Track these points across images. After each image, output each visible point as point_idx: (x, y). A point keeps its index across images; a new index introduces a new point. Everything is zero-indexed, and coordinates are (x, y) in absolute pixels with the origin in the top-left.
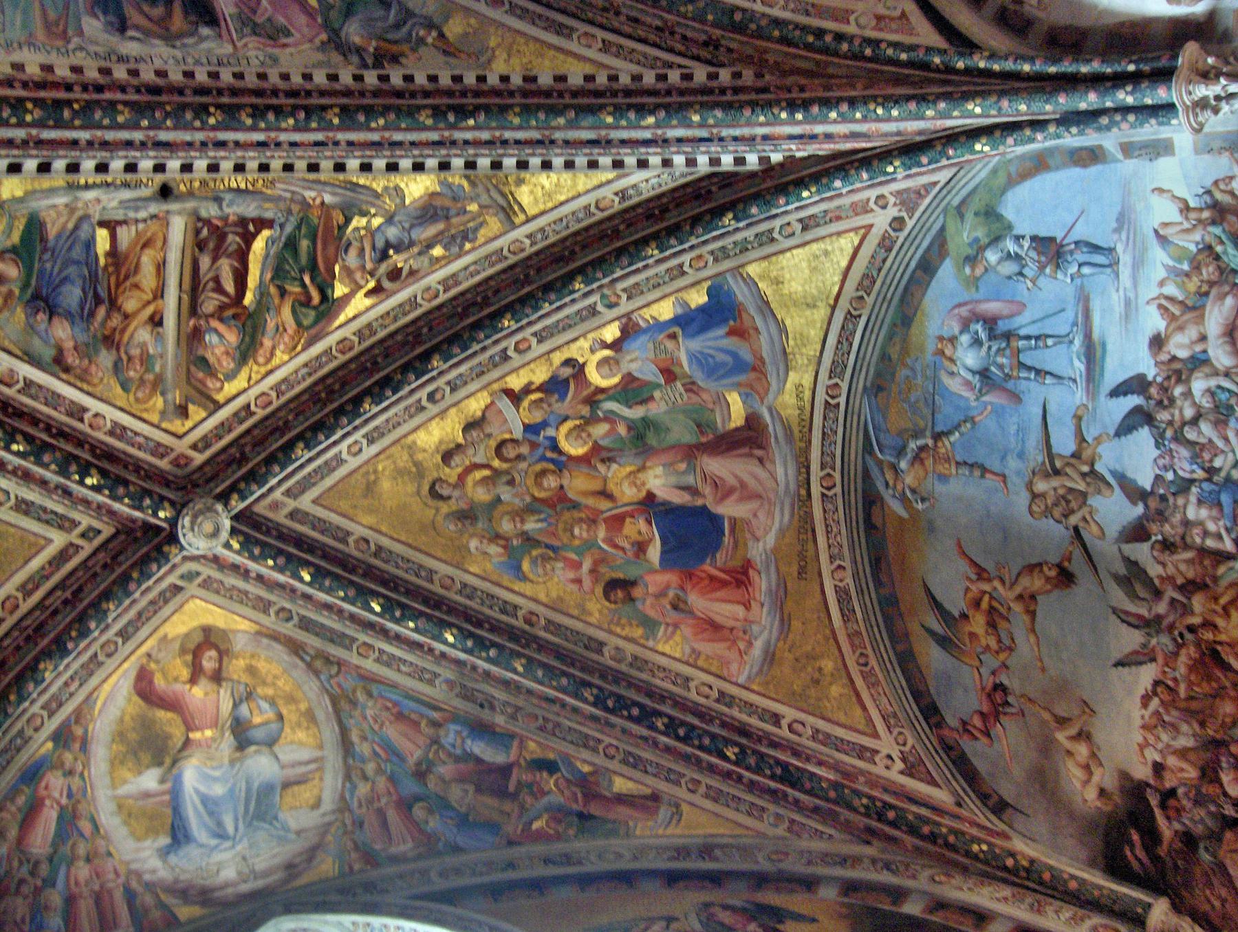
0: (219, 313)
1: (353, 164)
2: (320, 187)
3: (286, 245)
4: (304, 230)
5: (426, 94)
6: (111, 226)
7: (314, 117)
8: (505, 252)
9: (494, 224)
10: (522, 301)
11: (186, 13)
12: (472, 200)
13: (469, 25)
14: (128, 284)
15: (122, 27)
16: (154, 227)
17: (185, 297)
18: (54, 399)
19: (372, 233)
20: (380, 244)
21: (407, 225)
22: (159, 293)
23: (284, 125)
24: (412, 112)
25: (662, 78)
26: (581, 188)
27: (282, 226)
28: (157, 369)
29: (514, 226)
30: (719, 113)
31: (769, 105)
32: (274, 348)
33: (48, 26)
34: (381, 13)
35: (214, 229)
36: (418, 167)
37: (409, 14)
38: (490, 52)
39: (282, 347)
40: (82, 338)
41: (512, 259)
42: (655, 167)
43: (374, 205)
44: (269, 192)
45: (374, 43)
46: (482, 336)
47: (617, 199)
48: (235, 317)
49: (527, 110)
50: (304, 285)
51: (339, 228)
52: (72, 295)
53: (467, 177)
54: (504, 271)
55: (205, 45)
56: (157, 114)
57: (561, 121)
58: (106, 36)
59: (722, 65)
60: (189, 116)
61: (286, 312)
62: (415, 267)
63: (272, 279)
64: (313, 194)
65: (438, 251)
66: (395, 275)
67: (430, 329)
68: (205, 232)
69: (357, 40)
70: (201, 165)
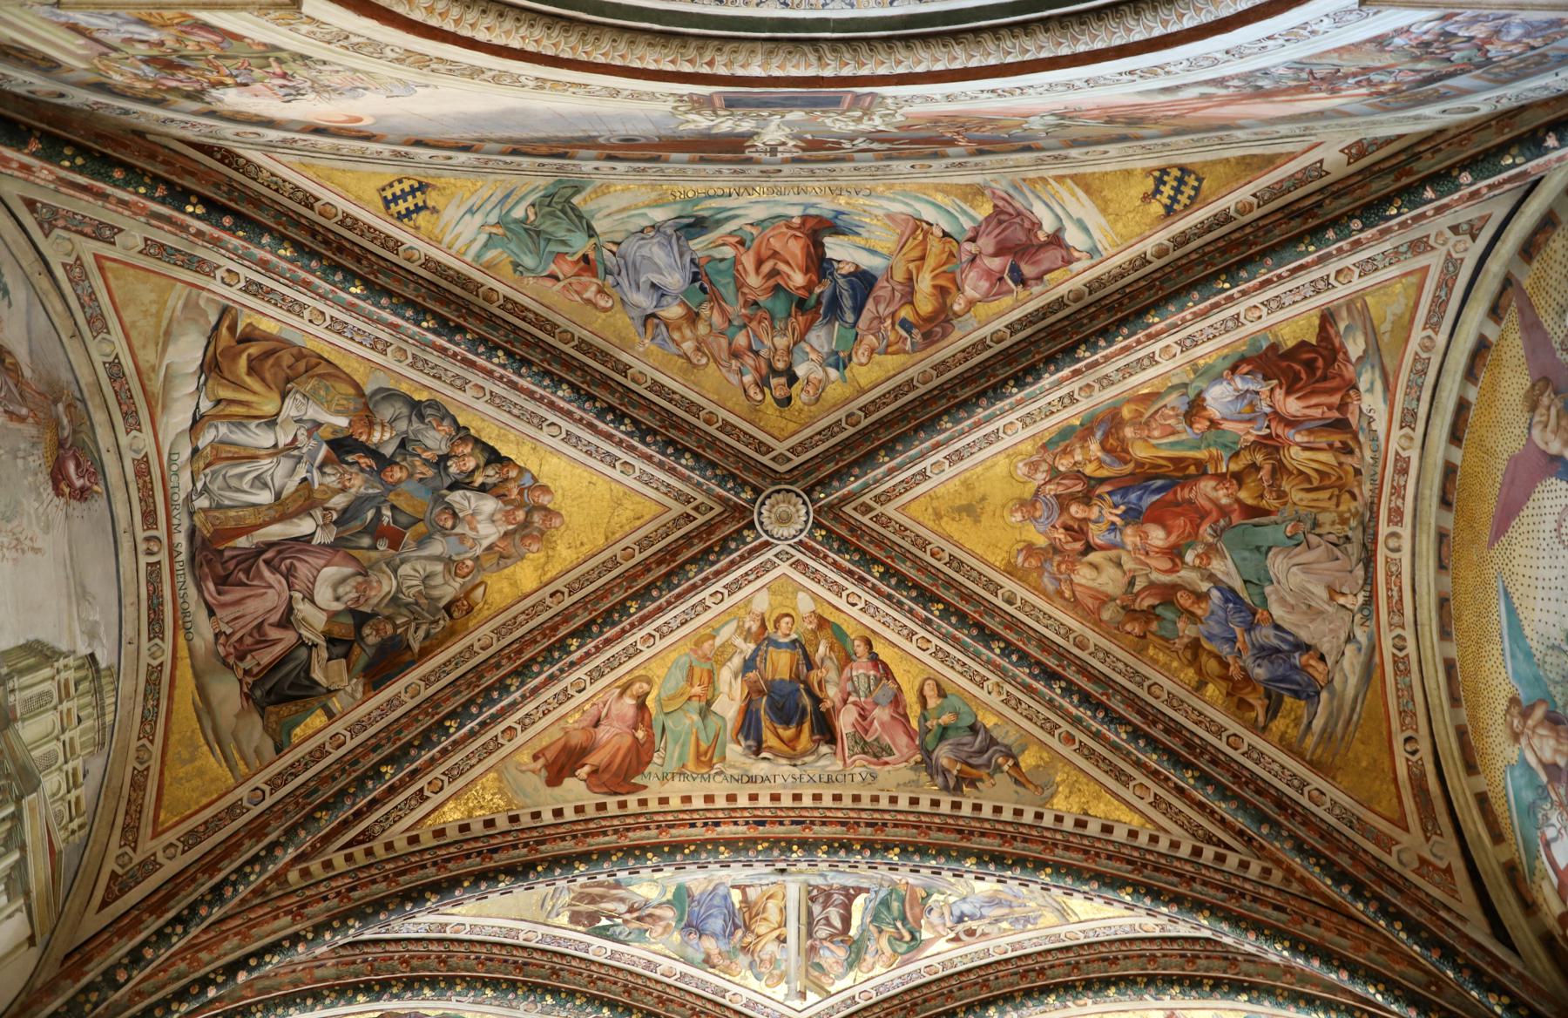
6: (742, 888)
9: (1050, 918)
11: (812, 732)
18: (704, 984)
19: (950, 906)
20: (957, 913)
22: (783, 924)
25: (1197, 852)
29: (1068, 922)
33: (698, 755)
34: (969, 739)
37: (992, 742)
40: (724, 948)
45: (959, 766)
52: (716, 924)
55: (822, 763)
58: (743, 759)
61: (884, 943)
65: (1004, 925)
66: (971, 933)
69: (944, 762)
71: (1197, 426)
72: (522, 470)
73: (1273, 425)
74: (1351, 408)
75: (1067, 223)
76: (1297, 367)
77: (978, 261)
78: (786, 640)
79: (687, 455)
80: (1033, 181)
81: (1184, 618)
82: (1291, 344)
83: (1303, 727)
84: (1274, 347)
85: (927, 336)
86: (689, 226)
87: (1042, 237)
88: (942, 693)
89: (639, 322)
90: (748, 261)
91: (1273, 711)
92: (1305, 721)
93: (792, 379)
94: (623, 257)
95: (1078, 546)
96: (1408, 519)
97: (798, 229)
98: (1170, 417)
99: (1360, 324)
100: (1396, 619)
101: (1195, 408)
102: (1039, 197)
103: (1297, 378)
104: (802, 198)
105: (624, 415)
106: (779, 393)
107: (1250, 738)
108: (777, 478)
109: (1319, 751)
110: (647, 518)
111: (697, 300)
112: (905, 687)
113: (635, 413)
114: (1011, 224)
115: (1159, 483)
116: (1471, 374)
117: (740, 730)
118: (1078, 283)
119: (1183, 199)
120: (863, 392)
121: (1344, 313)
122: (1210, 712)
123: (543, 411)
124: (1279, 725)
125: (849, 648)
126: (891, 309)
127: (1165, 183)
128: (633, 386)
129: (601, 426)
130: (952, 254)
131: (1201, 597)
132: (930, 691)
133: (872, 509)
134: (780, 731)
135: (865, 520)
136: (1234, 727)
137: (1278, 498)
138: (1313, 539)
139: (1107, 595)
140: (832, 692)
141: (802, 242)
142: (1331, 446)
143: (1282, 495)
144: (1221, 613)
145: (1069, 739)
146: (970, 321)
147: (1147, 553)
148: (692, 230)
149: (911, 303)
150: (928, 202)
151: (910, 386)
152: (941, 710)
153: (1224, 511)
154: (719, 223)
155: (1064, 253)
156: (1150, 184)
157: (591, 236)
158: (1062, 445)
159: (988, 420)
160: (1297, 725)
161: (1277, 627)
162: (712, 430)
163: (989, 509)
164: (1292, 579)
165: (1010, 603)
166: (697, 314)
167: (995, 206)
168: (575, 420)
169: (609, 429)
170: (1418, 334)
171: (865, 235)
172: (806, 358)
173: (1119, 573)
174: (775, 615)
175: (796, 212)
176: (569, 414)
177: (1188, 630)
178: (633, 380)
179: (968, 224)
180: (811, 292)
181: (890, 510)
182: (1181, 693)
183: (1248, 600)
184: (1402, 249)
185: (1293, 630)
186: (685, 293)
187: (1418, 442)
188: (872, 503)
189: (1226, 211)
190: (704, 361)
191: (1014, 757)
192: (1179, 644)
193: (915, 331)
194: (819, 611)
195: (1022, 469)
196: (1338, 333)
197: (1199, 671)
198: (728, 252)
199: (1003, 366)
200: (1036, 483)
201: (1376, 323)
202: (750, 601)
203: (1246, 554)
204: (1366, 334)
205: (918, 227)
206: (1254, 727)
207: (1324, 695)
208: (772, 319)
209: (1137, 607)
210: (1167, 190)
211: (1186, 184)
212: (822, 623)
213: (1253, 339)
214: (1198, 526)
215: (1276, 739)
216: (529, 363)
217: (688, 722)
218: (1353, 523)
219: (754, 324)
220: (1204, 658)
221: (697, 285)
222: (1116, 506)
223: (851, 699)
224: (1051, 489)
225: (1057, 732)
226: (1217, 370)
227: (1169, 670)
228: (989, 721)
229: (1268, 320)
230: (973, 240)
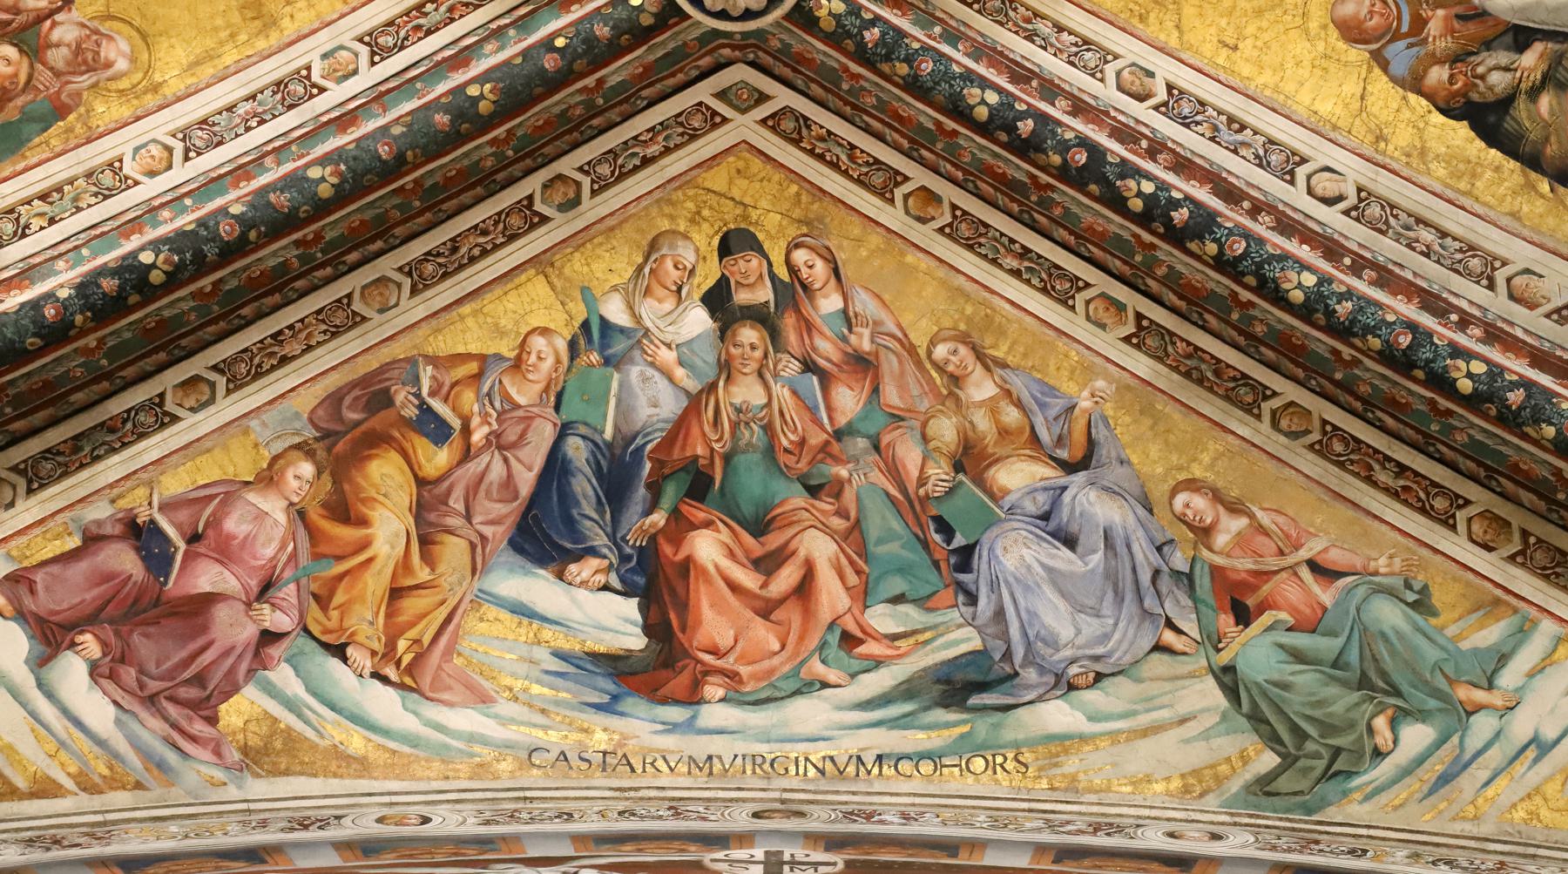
72: (1414, 83)
75: (24, 678)
77: (254, 584)
79: (982, 113)
85: (382, 400)
86: (983, 687)
87: (90, 643)
89: (1104, 452)
90: (832, 596)
93: (717, 300)
94: (1146, 614)
97: (710, 671)
102: (101, 743)
104: (701, 746)
105: (1143, 219)
108: (754, 50)
111: (958, 501)
113: (1115, 223)
114: (169, 675)
123: (1355, 234)
126: (474, 467)
128: (1120, 292)
129: (1203, 194)
130: (323, 601)
141: (701, 638)
146: (270, 436)
148: (973, 675)
149: (421, 482)
154: (906, 691)
155: (28, 602)
157: (1229, 669)
162: (920, 177)
166: (958, 467)
167: (213, 720)
168: (1271, 209)
169: (1182, 186)
171: (542, 654)
175: (715, 714)
176: (1287, 226)
178: (1120, 307)
179: (283, 675)
180: (675, 514)
186: (991, 522)
190: (941, 351)
193: (411, 412)
198: (882, 619)
199: (178, 320)
208: (771, 451)
216: (1388, 356)
219: (816, 438)
221: (959, 541)
230: (269, 637)
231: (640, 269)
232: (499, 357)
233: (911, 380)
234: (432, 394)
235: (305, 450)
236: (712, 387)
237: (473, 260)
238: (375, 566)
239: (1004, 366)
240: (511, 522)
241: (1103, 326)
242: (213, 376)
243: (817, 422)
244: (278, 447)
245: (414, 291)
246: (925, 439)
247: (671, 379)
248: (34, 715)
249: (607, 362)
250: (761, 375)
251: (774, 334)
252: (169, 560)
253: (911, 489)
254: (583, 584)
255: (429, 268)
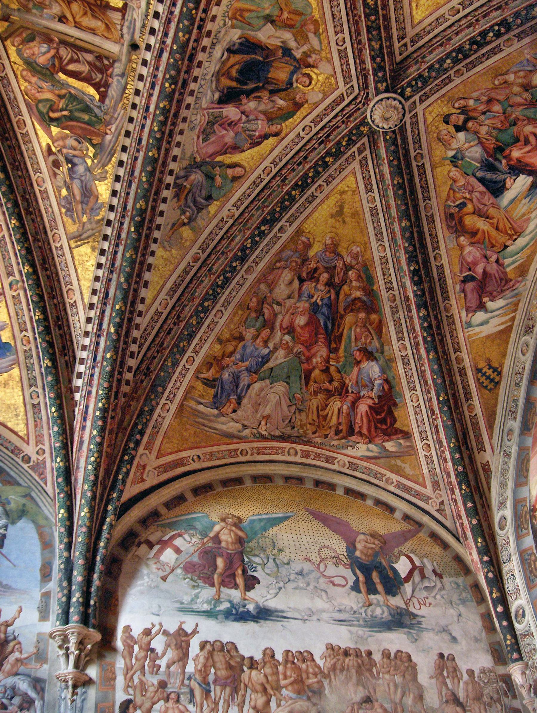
0: (57, 56)
1: (125, 157)
2: (116, 134)
3: (88, 106)
4: (94, 119)
5: (154, 208)
7: (155, 142)
8: (55, 231)
9: (73, 228)
10: (24, 234)
11: (229, 88)
12: (89, 219)
13: (186, 241)
14: (88, 9)
15: (230, 50)
16: (117, 34)
17: (72, 40)
19: (83, 158)
20: (76, 160)
21: (83, 178)
22: (78, 26)
23: (155, 124)
24: (146, 198)
25: (135, 341)
26: (82, 282)
27: (99, 107)
28: (34, 11)
30: (108, 369)
31: (108, 398)
32: (30, 82)
33: (242, 10)
34: (204, 195)
35: (107, 68)
36: (114, 193)
37: (200, 209)
38: (169, 249)
39: (29, 87)
41: (50, 234)
42: (86, 327)
43: (99, 162)
44: (120, 105)
45: (188, 186)
46: (9, 206)
47: (72, 302)
48: (54, 65)
49: (132, 262)
50: (62, 110)
51: (90, 140)
53: (103, 219)
54: (44, 228)
55: (209, 94)
56: (178, 56)
57: (122, 280)
58: (228, 40)
59: (135, 376)
60: (173, 73)
62: (58, 177)
63: (70, 93)
64: (113, 130)
65: (64, 192)
66: (56, 164)
67: (20, 177)
68: (106, 62)
69: (192, 177)
70: (144, 71)
71: (358, 353)
73: (353, 395)
74: (360, 438)
75: (488, 315)
76: (383, 414)
77: (484, 260)
78: (294, 79)
80: (517, 305)
81: (255, 332)
82: (396, 414)
83: (199, 399)
84: (395, 405)
85: (452, 216)
87: (485, 299)
88: (235, 179)
91: (207, 383)
92: (203, 401)
93: (458, 129)
95: (304, 275)
96: (304, 461)
98: (366, 340)
99: (402, 450)
100: (255, 451)
101: (369, 355)
102: (507, 304)
103: (378, 413)
106: (453, 118)
107: (193, 369)
109: (188, 409)
110: (414, 13)
112: (243, 155)
115: (330, 326)
116: (378, 502)
117: (247, 41)
118: (455, 311)
119: (483, 379)
120: (433, 168)
121: (408, 444)
122: (206, 346)
124: (199, 386)
125: (277, 121)
126: (475, 200)
127: (493, 372)
130: (493, 246)
131: (266, 343)
132: (238, 171)
133: (359, 154)
134: (237, 67)
135: (355, 149)
136: (198, 360)
137: (314, 391)
138: (293, 408)
139: (273, 289)
140: (252, 105)
142: (340, 424)
143: (316, 393)
144: (256, 354)
145: (196, 259)
147: (293, 314)
149: (474, 213)
150: (528, 244)
151: (427, 198)
152: (224, 177)
153: (309, 360)
155: (473, 309)
156: (495, 365)
158: (364, 276)
159: (393, 240)
160: (200, 396)
161: (249, 386)
163: (337, 225)
164: (272, 395)
165: (280, 230)
166: (527, 90)
167: (511, 280)
170: (395, 477)
171: (524, 201)
172: (467, 141)
173: (285, 297)
174: (314, 76)
177: (249, 334)
179: (507, 261)
180: (505, 157)
181: (355, 165)
182: (217, 330)
183: (262, 370)
184: (436, 477)
185: (248, 395)
187: (342, 470)
188: (363, 155)
189: (471, 399)
190: (497, 82)
191: (189, 222)
192: (242, 329)
193: (457, 209)
194: (306, 106)
195: (356, 249)
196: (398, 438)
197: (228, 340)
200: (345, 256)
201: (402, 458)
202: (329, 61)
203: (286, 370)
204: (396, 452)
205: (516, 233)
206: (198, 371)
207: (216, 411)
209: (265, 305)
210: (489, 372)
211: (490, 383)
212: (298, 106)
213: (402, 395)
214: (303, 344)
215: (193, 384)
217: (266, 6)
218: (301, 431)
219: (502, 118)
220: (234, 343)
222: (322, 300)
223: (244, 117)
224: (340, 264)
225: (200, 251)
226: (388, 373)
227: (229, 323)
228: (212, 209)
229: (410, 405)
230: (497, 261)
231: (443, 144)
232: (451, 185)
233: (501, 92)
234: (454, 203)
235: (457, 237)
236: (479, 138)
237: (427, 184)
238: (490, 232)
239: (508, 70)
240: (490, 195)
241: (512, 45)
242: (435, 253)
243: (498, 117)
244: (455, 243)
245: (430, 200)
246: (516, 95)
247: (472, 146)
248: (497, 316)
249: (462, 159)
250: (481, 125)
251: (472, 118)
252: (473, 277)
253: (525, 102)
254: (512, 185)
255: (426, 195)
